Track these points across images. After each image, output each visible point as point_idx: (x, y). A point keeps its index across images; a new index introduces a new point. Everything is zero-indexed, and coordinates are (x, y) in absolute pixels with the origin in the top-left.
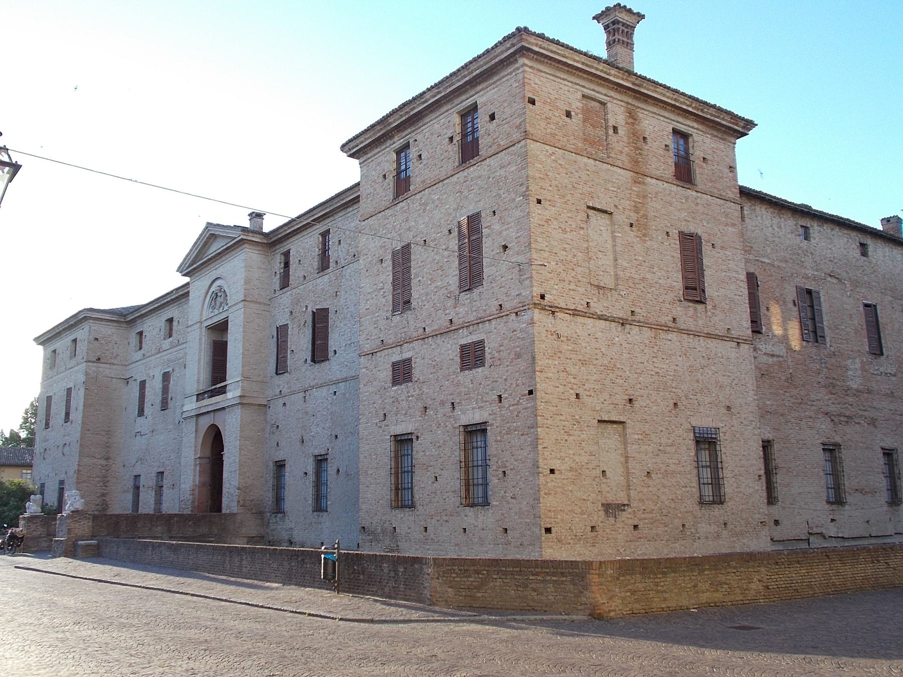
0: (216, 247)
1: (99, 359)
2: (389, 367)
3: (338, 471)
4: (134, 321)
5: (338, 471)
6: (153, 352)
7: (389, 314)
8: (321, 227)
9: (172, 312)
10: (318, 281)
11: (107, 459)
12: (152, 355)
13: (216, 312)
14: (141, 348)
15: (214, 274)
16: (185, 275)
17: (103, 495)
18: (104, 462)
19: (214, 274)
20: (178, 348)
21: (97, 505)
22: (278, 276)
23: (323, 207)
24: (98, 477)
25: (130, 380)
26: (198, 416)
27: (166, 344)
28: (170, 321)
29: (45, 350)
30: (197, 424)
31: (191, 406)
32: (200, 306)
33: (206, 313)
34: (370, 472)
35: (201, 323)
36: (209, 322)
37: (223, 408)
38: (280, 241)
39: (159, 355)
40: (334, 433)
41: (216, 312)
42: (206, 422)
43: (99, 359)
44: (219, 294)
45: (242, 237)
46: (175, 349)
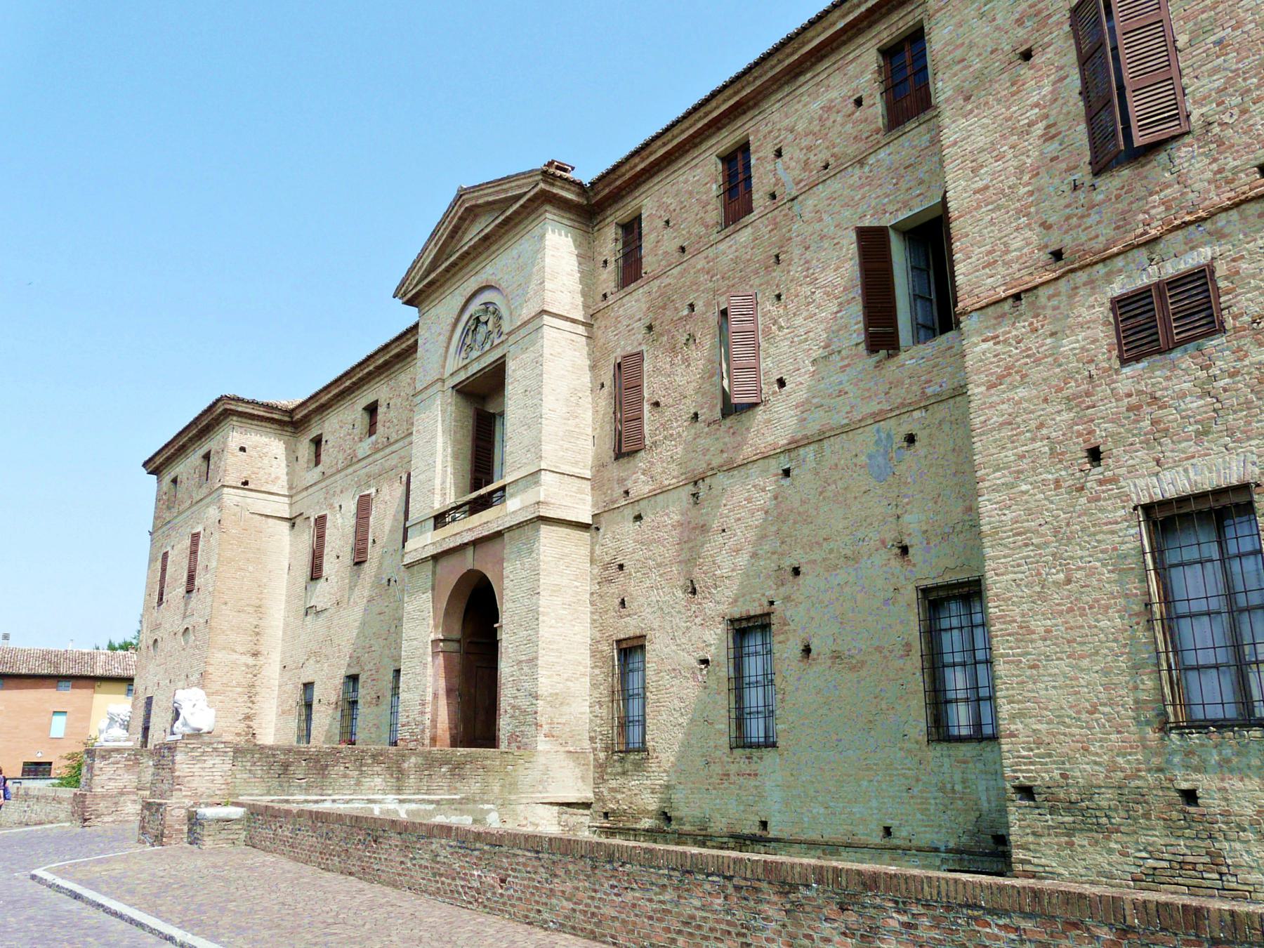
0: (473, 234)
1: (246, 483)
2: (1102, 311)
3: (807, 650)
4: (306, 419)
5: (807, 650)
6: (340, 466)
7: (1083, 173)
8: (725, 140)
9: (379, 391)
10: (722, 246)
11: (255, 655)
12: (339, 471)
13: (475, 354)
14: (317, 463)
15: (472, 284)
16: (410, 302)
17: (248, 717)
18: (251, 661)
19: (472, 284)
20: (388, 451)
21: (238, 734)
22: (611, 266)
23: (738, 85)
24: (239, 685)
25: (298, 521)
26: (436, 558)
27: (365, 447)
28: (372, 409)
29: (159, 481)
30: (434, 573)
31: (425, 542)
32: (442, 351)
33: (453, 363)
34: (1038, 625)
35: (443, 381)
36: (457, 380)
37: (499, 534)
38: (617, 196)
39: (350, 470)
40: (788, 563)
41: (475, 354)
42: (453, 571)
43: (246, 483)
44: (483, 319)
45: (542, 185)
46: (382, 453)
